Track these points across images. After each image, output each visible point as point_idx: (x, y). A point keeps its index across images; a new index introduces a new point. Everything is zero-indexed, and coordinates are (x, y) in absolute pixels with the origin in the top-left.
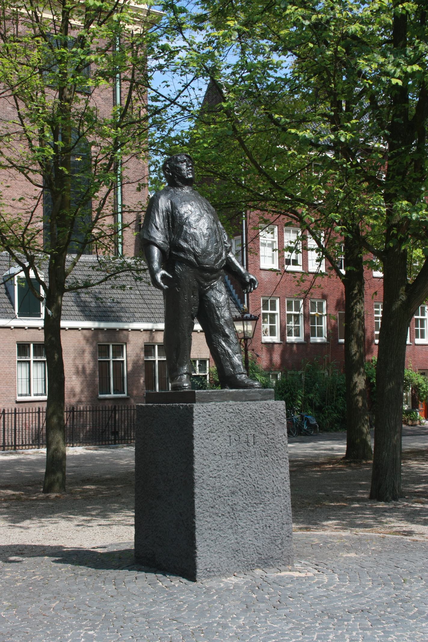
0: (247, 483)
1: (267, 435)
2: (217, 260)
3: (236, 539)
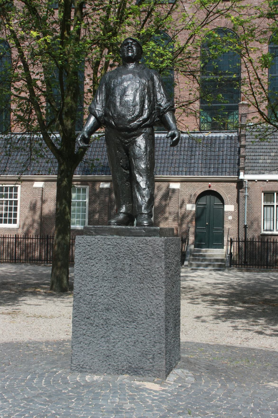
0: (122, 303)
1: (143, 266)
2: (133, 120)
3: (108, 346)
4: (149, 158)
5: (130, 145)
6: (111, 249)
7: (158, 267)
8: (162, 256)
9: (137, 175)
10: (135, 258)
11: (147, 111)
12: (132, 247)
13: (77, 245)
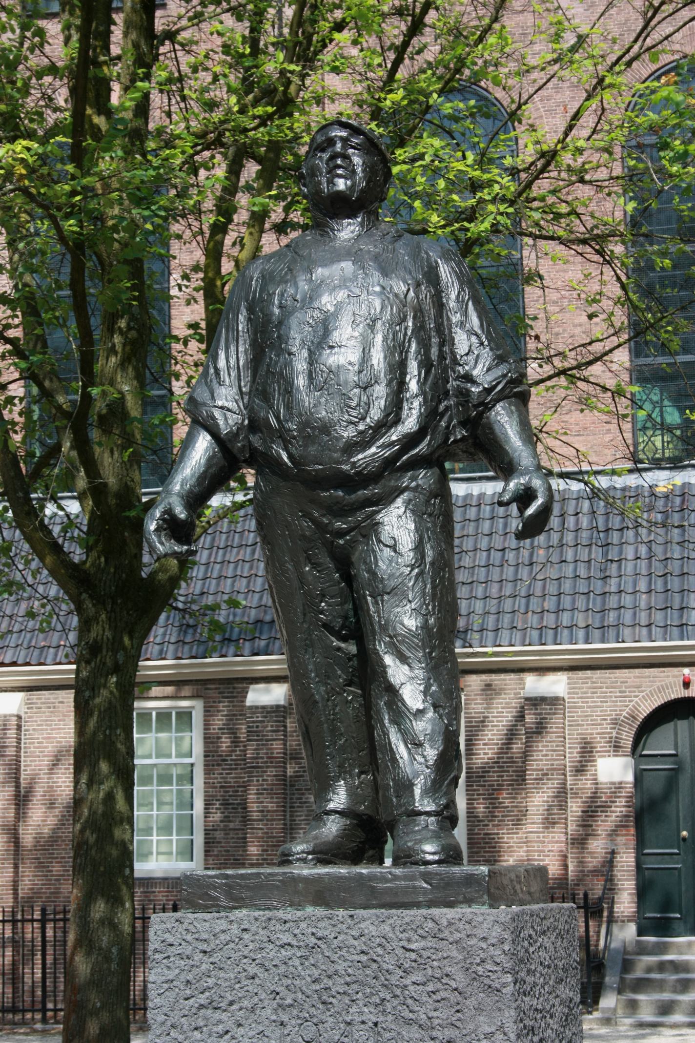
2: (363, 442)
4: (434, 587)
5: (354, 542)
6: (297, 962)
7: (488, 1030)
8: (505, 985)
9: (388, 660)
10: (395, 996)
11: (416, 404)
12: (380, 951)
13: (156, 951)
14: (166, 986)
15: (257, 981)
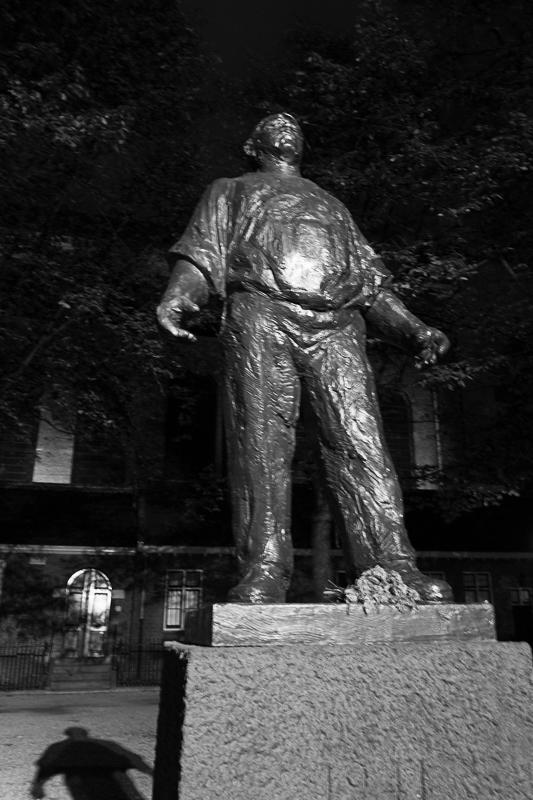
14: (204, 729)
15: (303, 720)
